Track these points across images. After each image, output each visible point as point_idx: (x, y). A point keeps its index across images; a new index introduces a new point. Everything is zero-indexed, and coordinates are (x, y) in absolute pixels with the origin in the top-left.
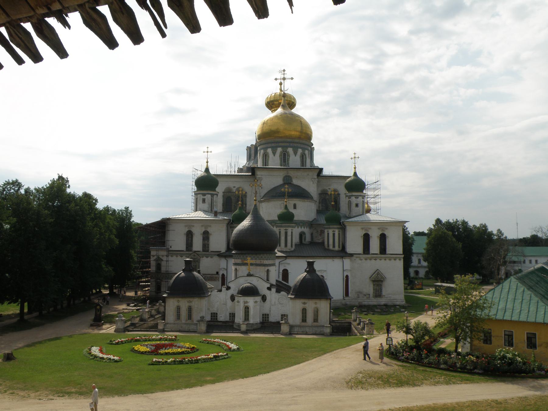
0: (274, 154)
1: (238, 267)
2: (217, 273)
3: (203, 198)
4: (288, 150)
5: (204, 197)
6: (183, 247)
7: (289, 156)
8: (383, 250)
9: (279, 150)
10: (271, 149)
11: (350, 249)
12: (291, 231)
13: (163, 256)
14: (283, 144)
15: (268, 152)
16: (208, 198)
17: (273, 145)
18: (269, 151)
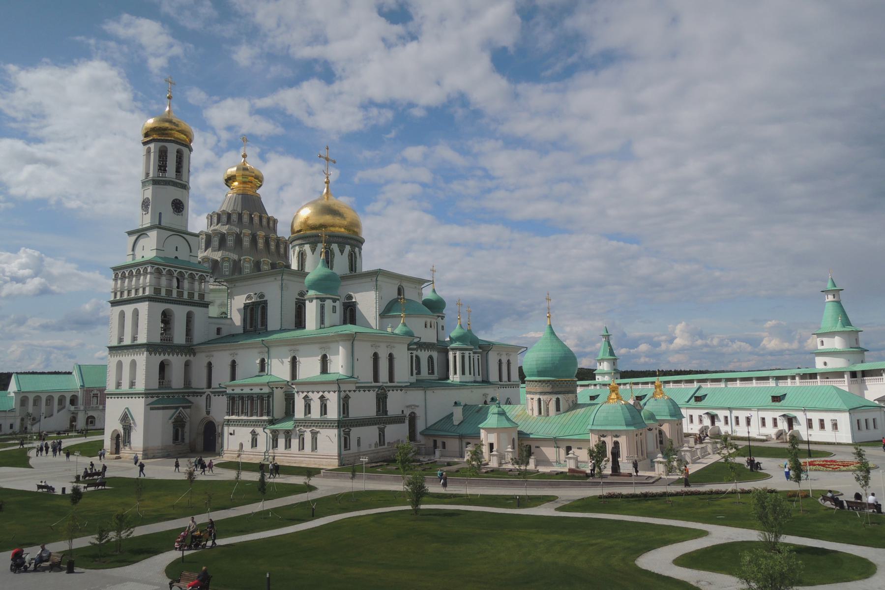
0: (342, 252)
1: (560, 396)
2: (403, 411)
3: (333, 306)
4: (356, 250)
5: (334, 304)
6: (366, 375)
7: (356, 257)
8: (509, 380)
9: (348, 248)
10: (336, 245)
11: (491, 380)
12: (477, 358)
13: (350, 391)
14: (352, 242)
15: (332, 248)
16: (337, 304)
17: (340, 240)
18: (335, 247)
